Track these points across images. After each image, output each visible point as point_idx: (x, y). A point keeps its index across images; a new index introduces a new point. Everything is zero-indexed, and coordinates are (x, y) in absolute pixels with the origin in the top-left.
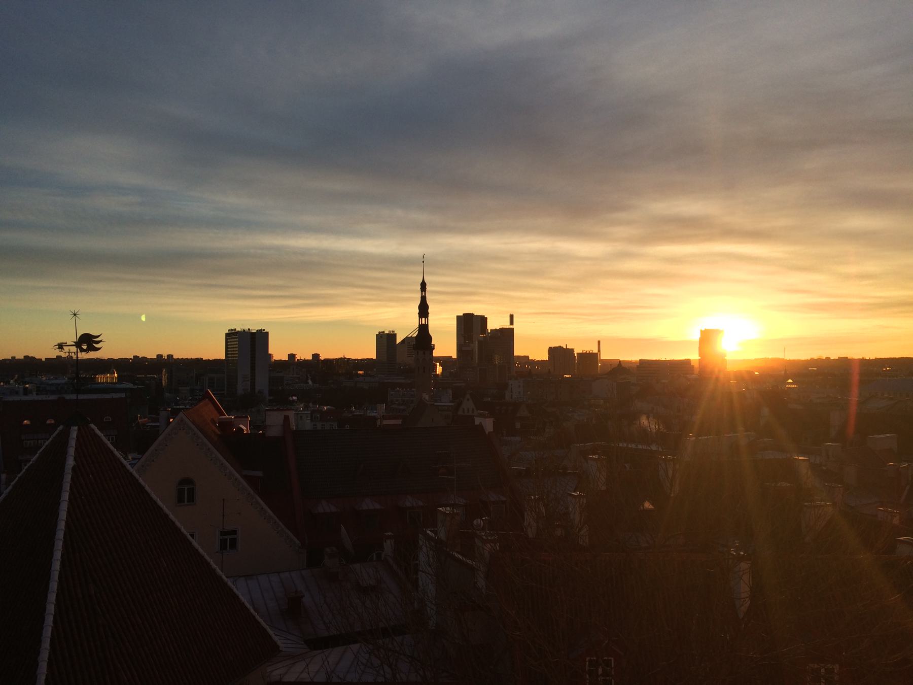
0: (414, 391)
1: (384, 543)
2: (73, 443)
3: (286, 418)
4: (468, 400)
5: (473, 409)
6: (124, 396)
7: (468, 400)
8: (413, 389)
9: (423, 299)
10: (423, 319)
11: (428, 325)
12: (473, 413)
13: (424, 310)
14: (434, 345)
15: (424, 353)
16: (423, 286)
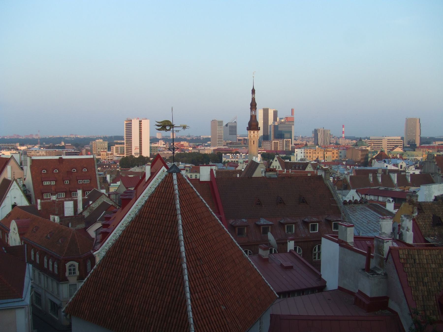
0: (238, 156)
1: (288, 242)
2: (175, 182)
3: (212, 170)
4: (276, 161)
5: (279, 167)
6: (93, 157)
7: (276, 161)
8: (237, 154)
9: (253, 100)
10: (253, 112)
11: (256, 116)
12: (279, 168)
13: (253, 105)
14: (260, 127)
15: (254, 133)
16: (253, 91)
